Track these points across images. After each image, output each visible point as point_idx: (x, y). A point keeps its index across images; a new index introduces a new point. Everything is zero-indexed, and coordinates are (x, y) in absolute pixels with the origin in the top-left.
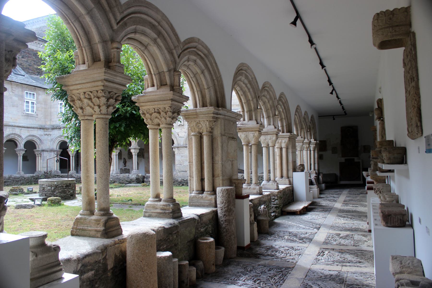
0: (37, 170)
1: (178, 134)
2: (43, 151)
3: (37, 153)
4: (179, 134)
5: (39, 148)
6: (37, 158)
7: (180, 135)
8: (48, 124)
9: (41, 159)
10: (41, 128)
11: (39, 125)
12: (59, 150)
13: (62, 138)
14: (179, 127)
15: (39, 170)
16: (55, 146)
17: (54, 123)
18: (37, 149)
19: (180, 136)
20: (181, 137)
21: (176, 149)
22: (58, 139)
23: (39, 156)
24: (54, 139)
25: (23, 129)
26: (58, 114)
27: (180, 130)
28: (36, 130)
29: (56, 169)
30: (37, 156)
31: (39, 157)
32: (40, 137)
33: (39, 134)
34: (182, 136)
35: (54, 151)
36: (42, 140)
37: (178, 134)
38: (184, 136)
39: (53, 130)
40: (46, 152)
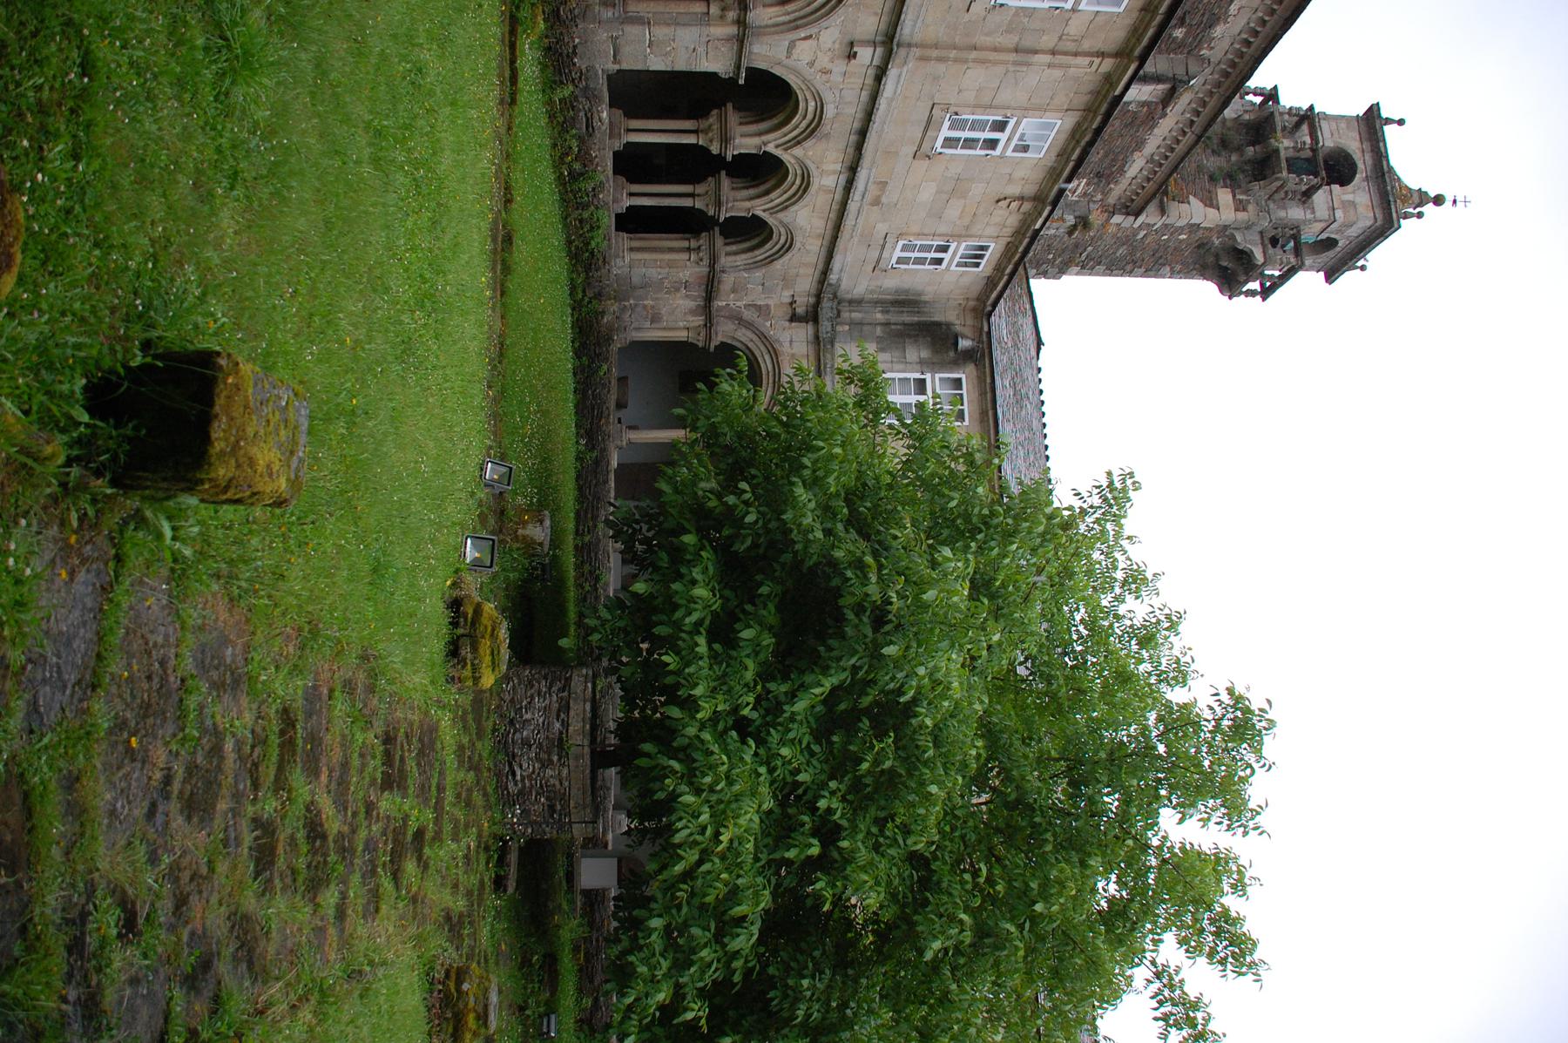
20: (792, 45)
21: (733, 30)
34: (796, 53)
38: (795, 56)
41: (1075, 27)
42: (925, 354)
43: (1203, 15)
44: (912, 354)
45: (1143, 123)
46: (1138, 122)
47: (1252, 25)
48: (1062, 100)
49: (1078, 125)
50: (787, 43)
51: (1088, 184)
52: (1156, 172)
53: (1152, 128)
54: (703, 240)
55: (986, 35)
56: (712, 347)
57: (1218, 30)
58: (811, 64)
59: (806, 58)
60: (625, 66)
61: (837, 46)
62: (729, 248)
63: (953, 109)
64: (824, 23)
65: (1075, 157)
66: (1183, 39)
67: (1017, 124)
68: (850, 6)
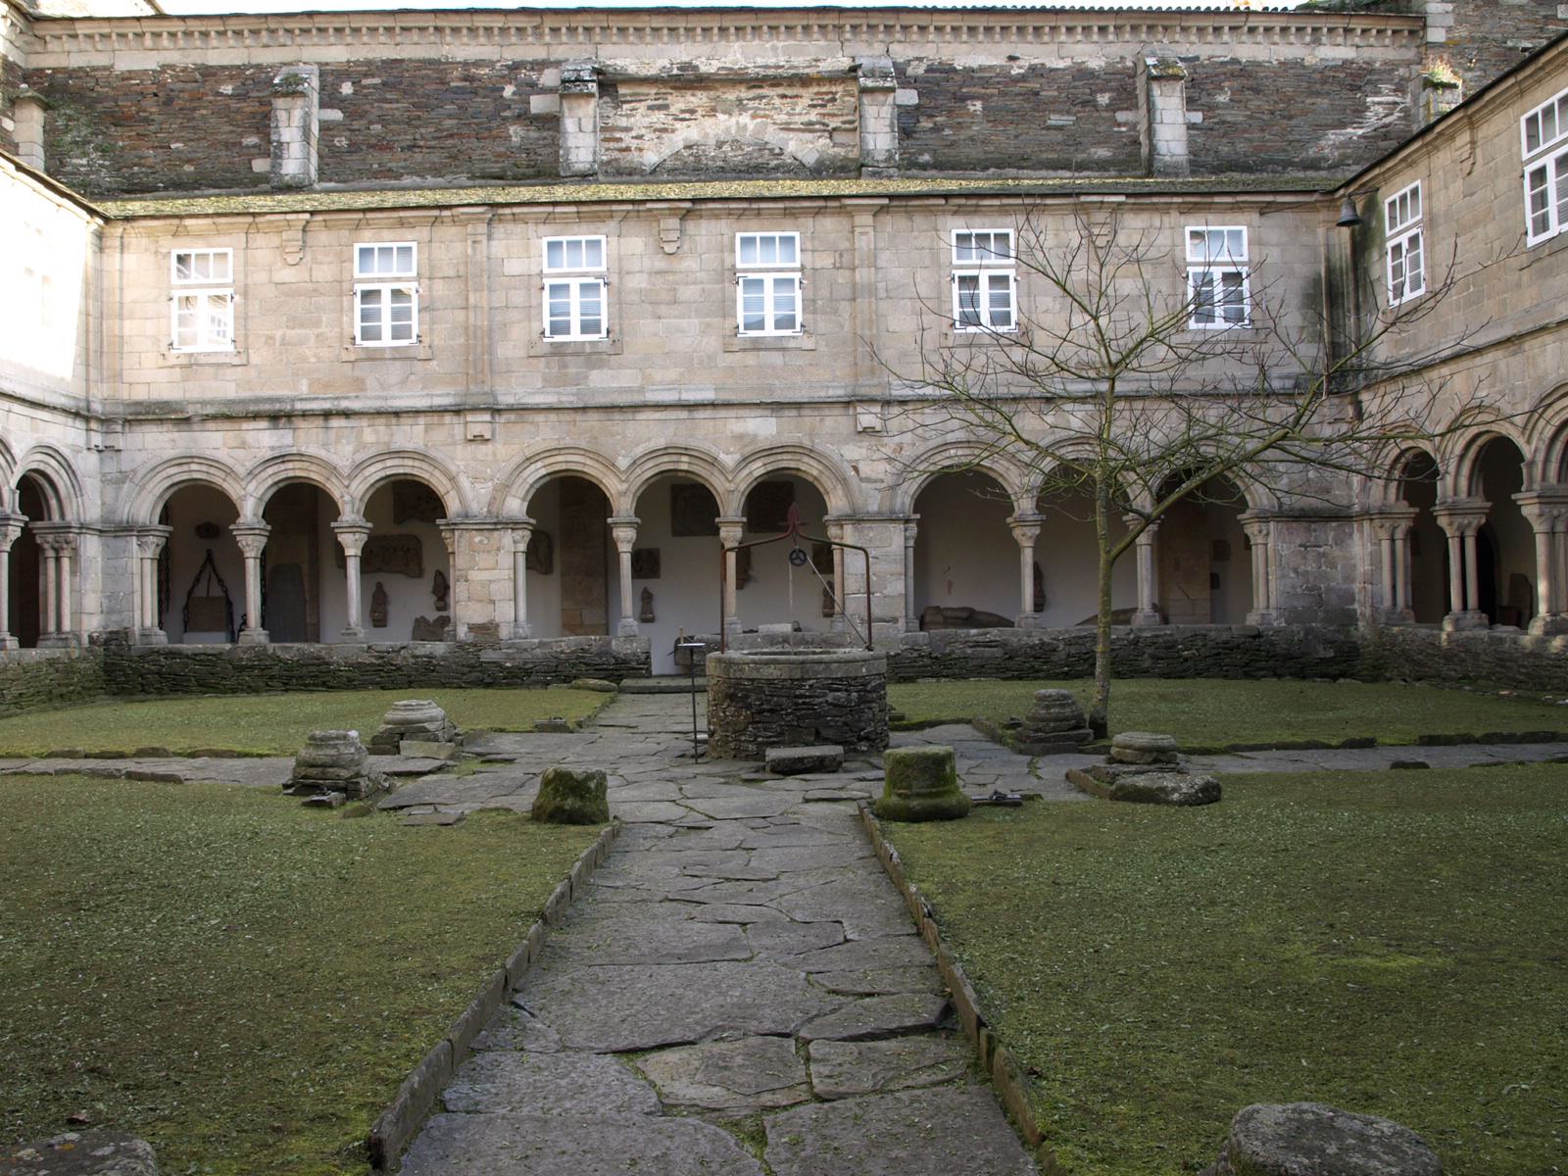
0: (52, 627)
1: (856, 469)
2: (84, 528)
3: (50, 538)
4: (861, 466)
5: (62, 516)
6: (51, 564)
7: (865, 470)
8: (100, 398)
9: (73, 573)
10: (81, 414)
11: (67, 396)
12: (161, 527)
13: (194, 467)
14: (857, 438)
15: (67, 626)
16: (145, 507)
17: (140, 394)
18: (56, 518)
19: (862, 475)
20: (868, 480)
22: (164, 474)
23: (66, 553)
24: (144, 471)
25: (17, 407)
26: (164, 348)
27: (864, 451)
28: (60, 418)
29: (148, 623)
30: (51, 553)
31: (66, 563)
32: (72, 461)
33: (70, 441)
34: (874, 476)
35: (143, 531)
36: (78, 473)
37: (856, 469)
38: (881, 476)
39: (136, 428)
40: (95, 538)
41: (826, 261)
42: (1375, 256)
43: (1075, 87)
44: (1375, 273)
45: (1250, 76)
46: (1251, 82)
47: (1079, 37)
48: (924, 240)
49: (955, 213)
50: (864, 485)
51: (1377, 93)
52: (1330, 30)
53: (1259, 64)
54: (1252, 529)
55: (842, 326)
56: (1412, 510)
57: (1095, 63)
58: (890, 460)
59: (884, 466)
60: (900, 612)
61: (866, 444)
62: (1250, 504)
63: (945, 329)
64: (836, 458)
65: (996, 202)
66: (1111, 90)
67: (961, 267)
68: (813, 442)
